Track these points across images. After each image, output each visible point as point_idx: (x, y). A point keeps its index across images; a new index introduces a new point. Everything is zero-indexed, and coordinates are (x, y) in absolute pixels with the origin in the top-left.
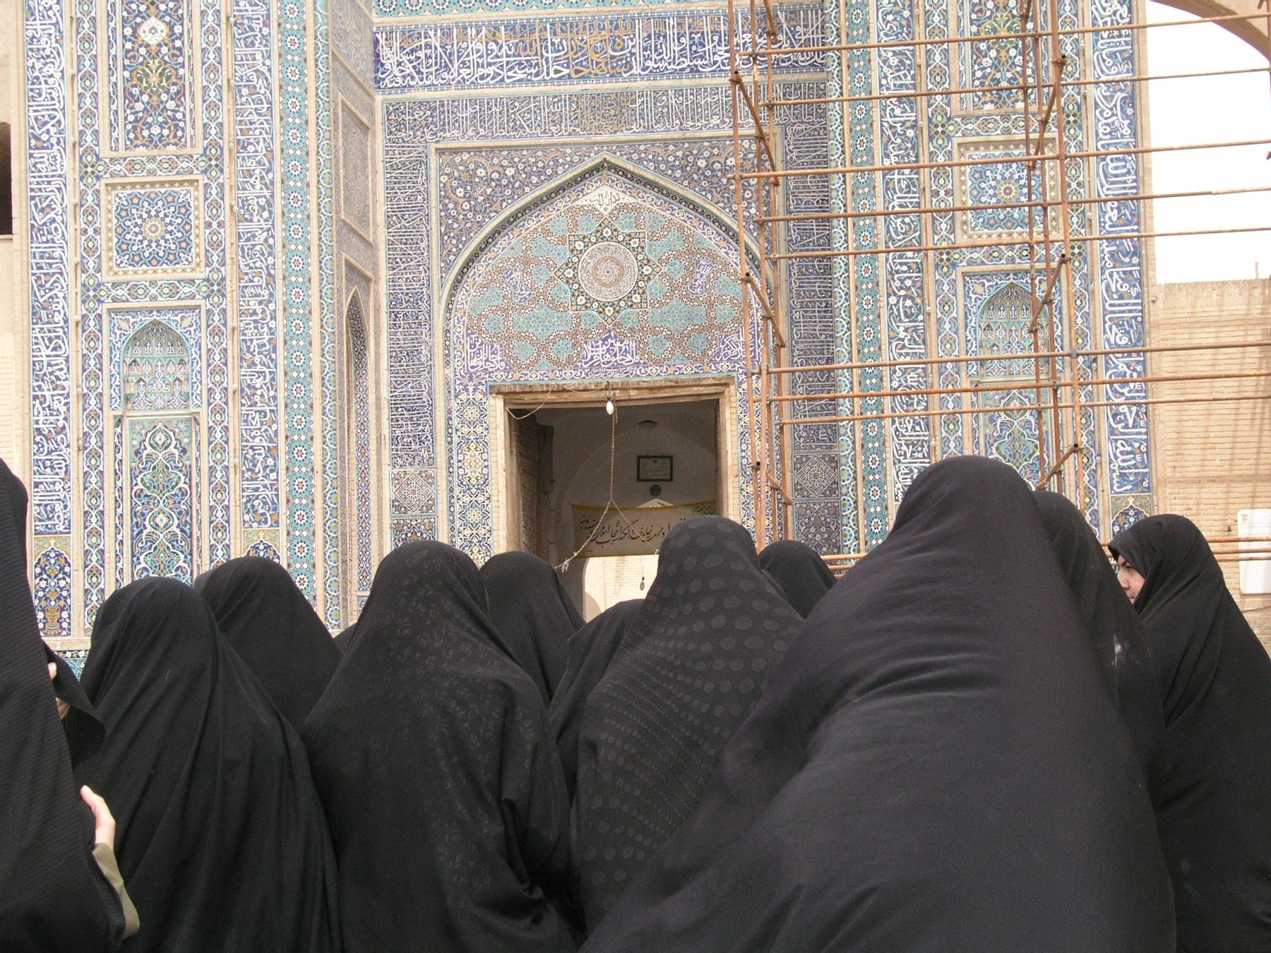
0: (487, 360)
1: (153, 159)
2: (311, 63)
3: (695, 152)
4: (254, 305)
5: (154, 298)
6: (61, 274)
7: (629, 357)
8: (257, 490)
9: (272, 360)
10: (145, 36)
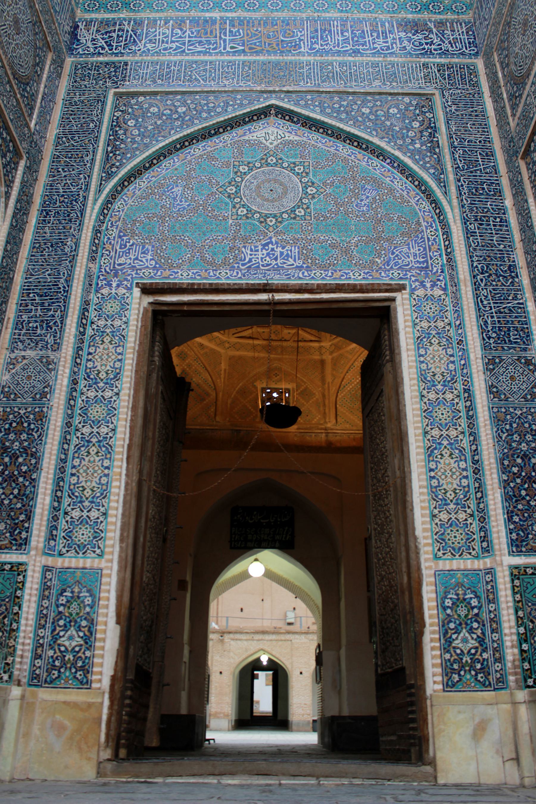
0: (137, 259)
3: (359, 103)
7: (291, 261)
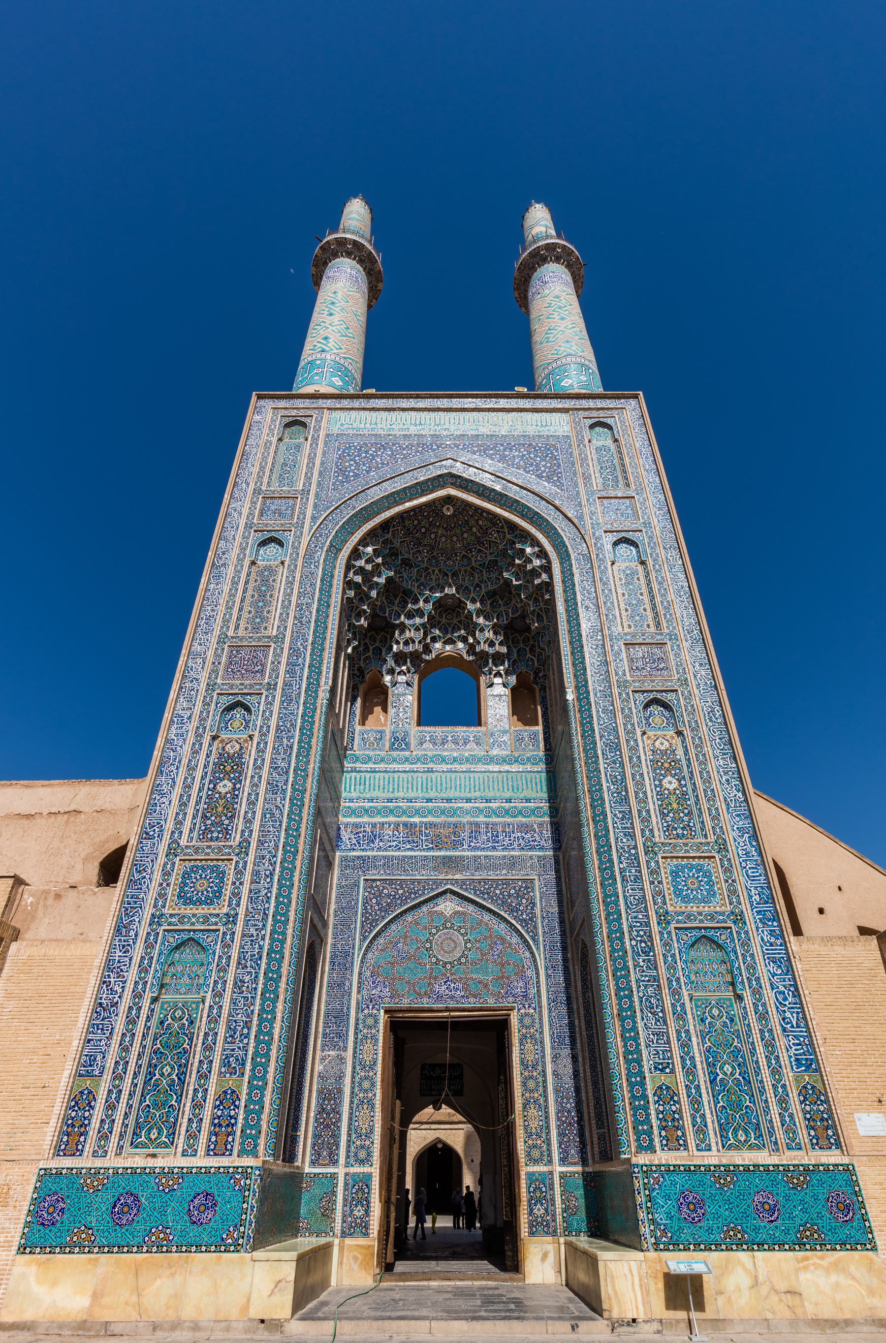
1: (210, 847)
2: (306, 807)
4: (252, 931)
5: (193, 924)
6: (141, 908)
8: (233, 1050)
9: (258, 964)
10: (220, 788)
